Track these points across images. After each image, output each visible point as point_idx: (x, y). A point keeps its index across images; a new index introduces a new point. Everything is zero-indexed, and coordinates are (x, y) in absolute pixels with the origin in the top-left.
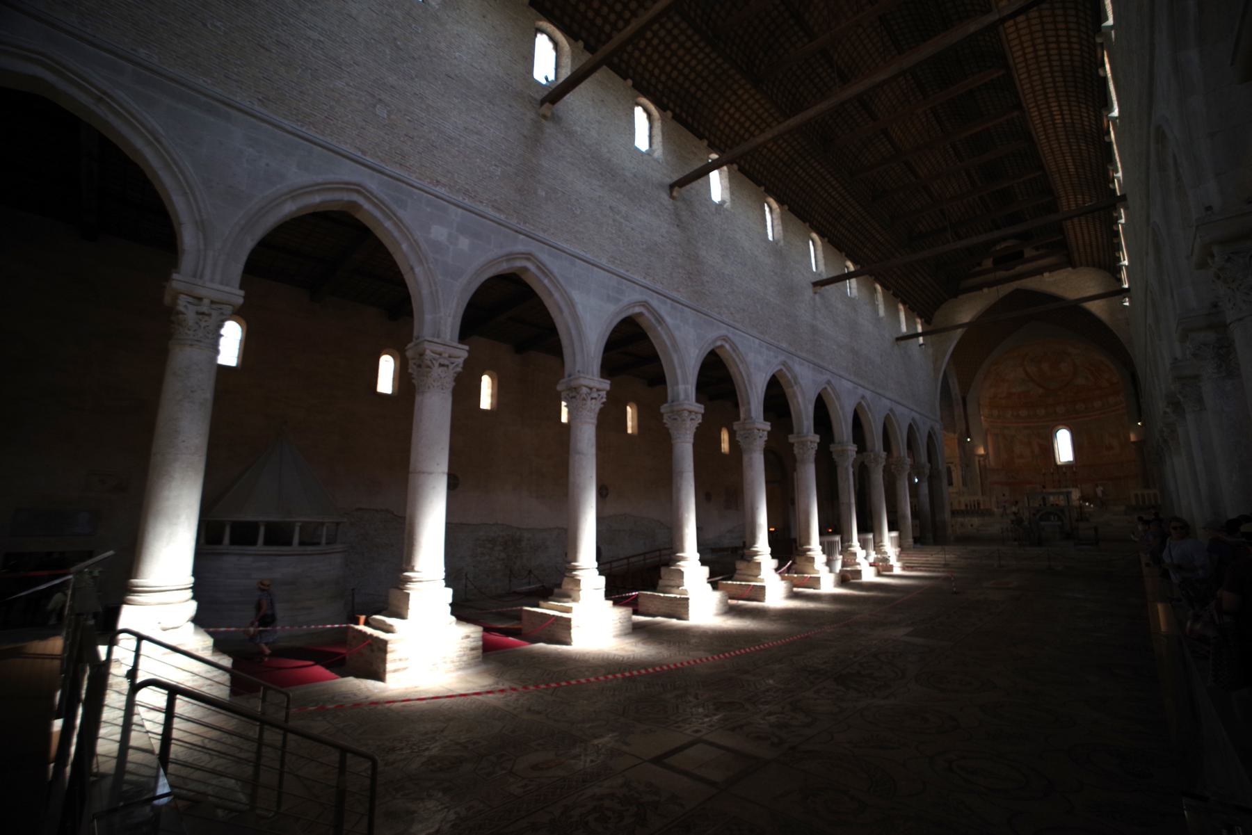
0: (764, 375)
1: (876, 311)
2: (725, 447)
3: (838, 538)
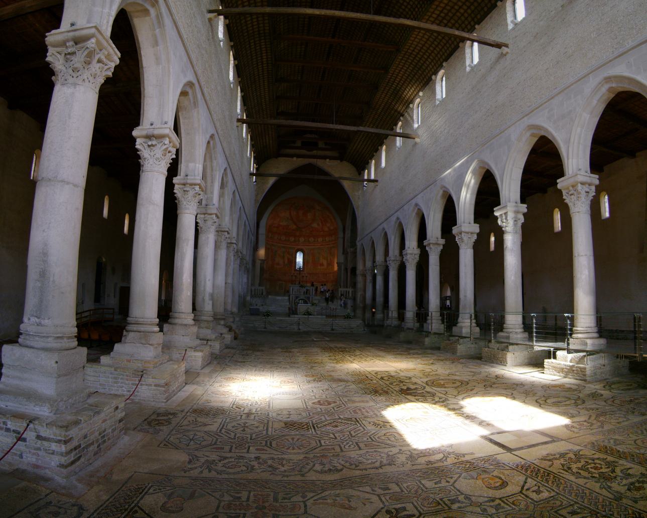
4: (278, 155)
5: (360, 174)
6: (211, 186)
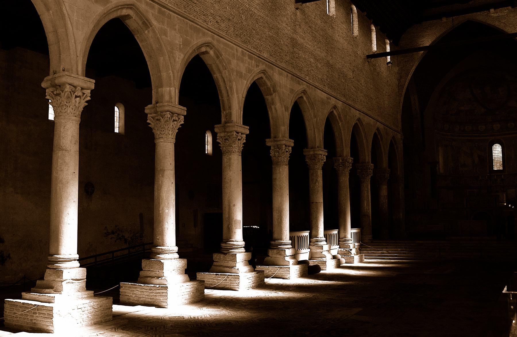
0: (246, 82)
1: (351, 30)
2: (209, 148)
3: (306, 234)
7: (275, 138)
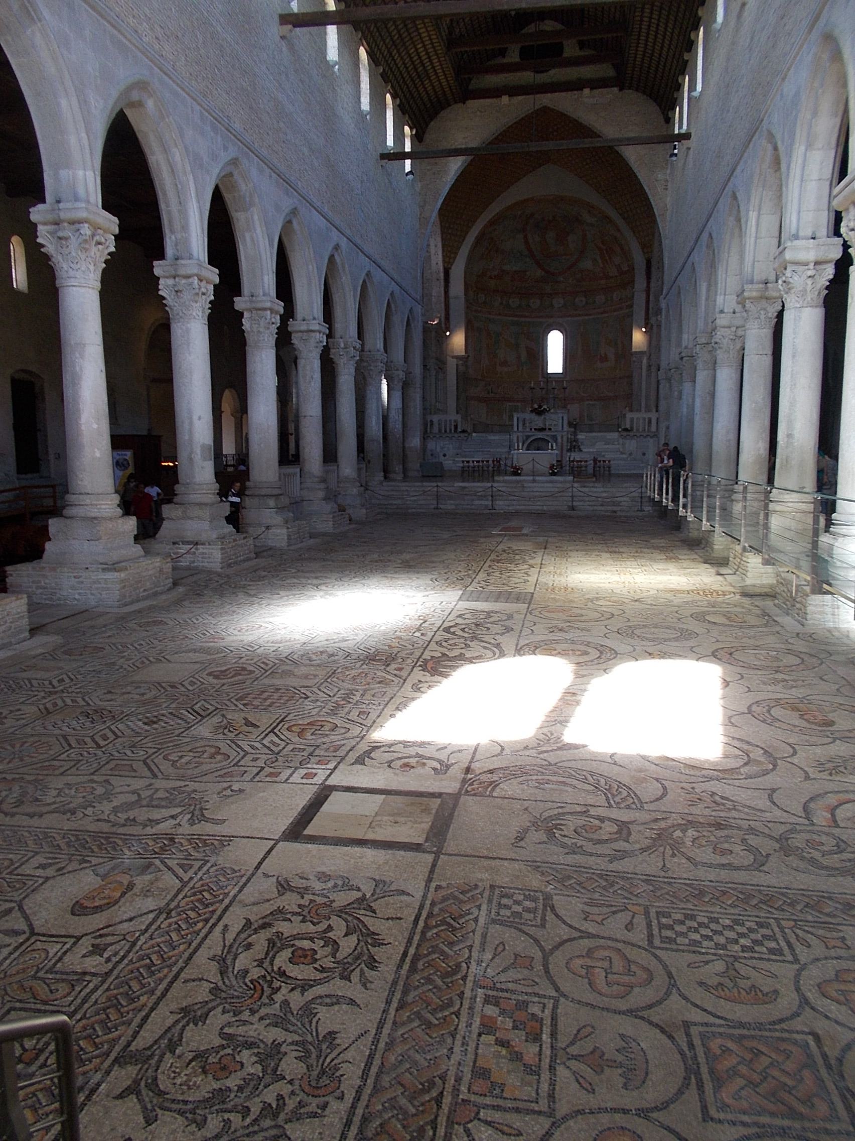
4: (466, 95)
5: (669, 120)
6: (179, 211)
7: (252, 296)
